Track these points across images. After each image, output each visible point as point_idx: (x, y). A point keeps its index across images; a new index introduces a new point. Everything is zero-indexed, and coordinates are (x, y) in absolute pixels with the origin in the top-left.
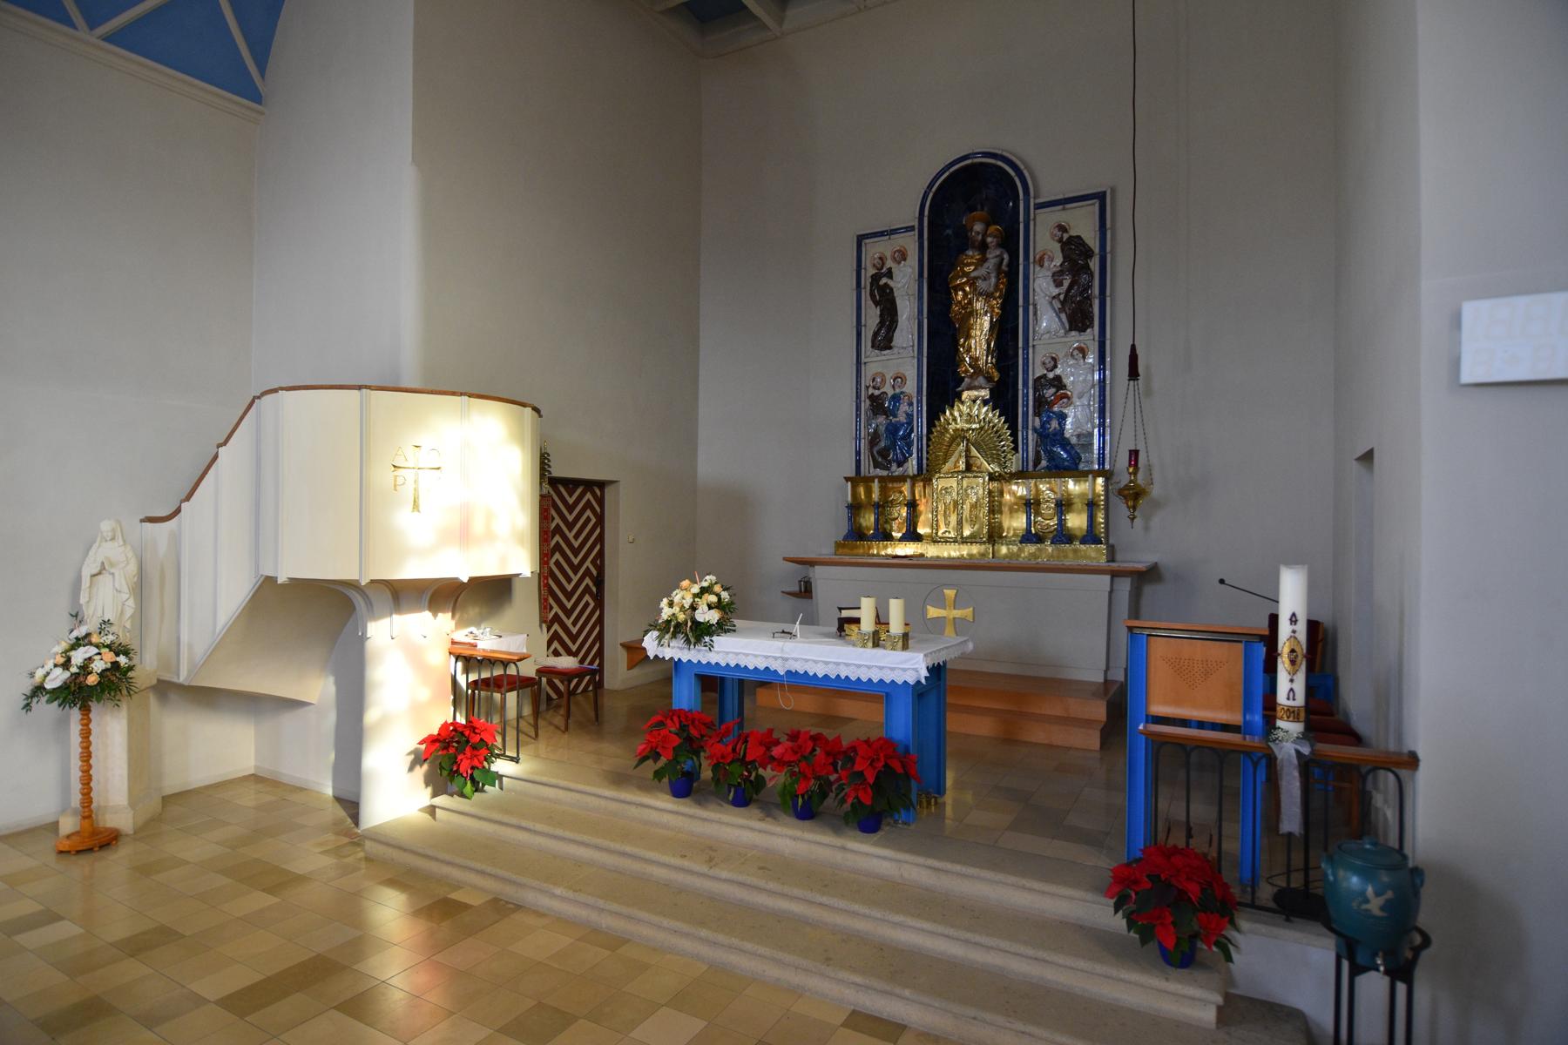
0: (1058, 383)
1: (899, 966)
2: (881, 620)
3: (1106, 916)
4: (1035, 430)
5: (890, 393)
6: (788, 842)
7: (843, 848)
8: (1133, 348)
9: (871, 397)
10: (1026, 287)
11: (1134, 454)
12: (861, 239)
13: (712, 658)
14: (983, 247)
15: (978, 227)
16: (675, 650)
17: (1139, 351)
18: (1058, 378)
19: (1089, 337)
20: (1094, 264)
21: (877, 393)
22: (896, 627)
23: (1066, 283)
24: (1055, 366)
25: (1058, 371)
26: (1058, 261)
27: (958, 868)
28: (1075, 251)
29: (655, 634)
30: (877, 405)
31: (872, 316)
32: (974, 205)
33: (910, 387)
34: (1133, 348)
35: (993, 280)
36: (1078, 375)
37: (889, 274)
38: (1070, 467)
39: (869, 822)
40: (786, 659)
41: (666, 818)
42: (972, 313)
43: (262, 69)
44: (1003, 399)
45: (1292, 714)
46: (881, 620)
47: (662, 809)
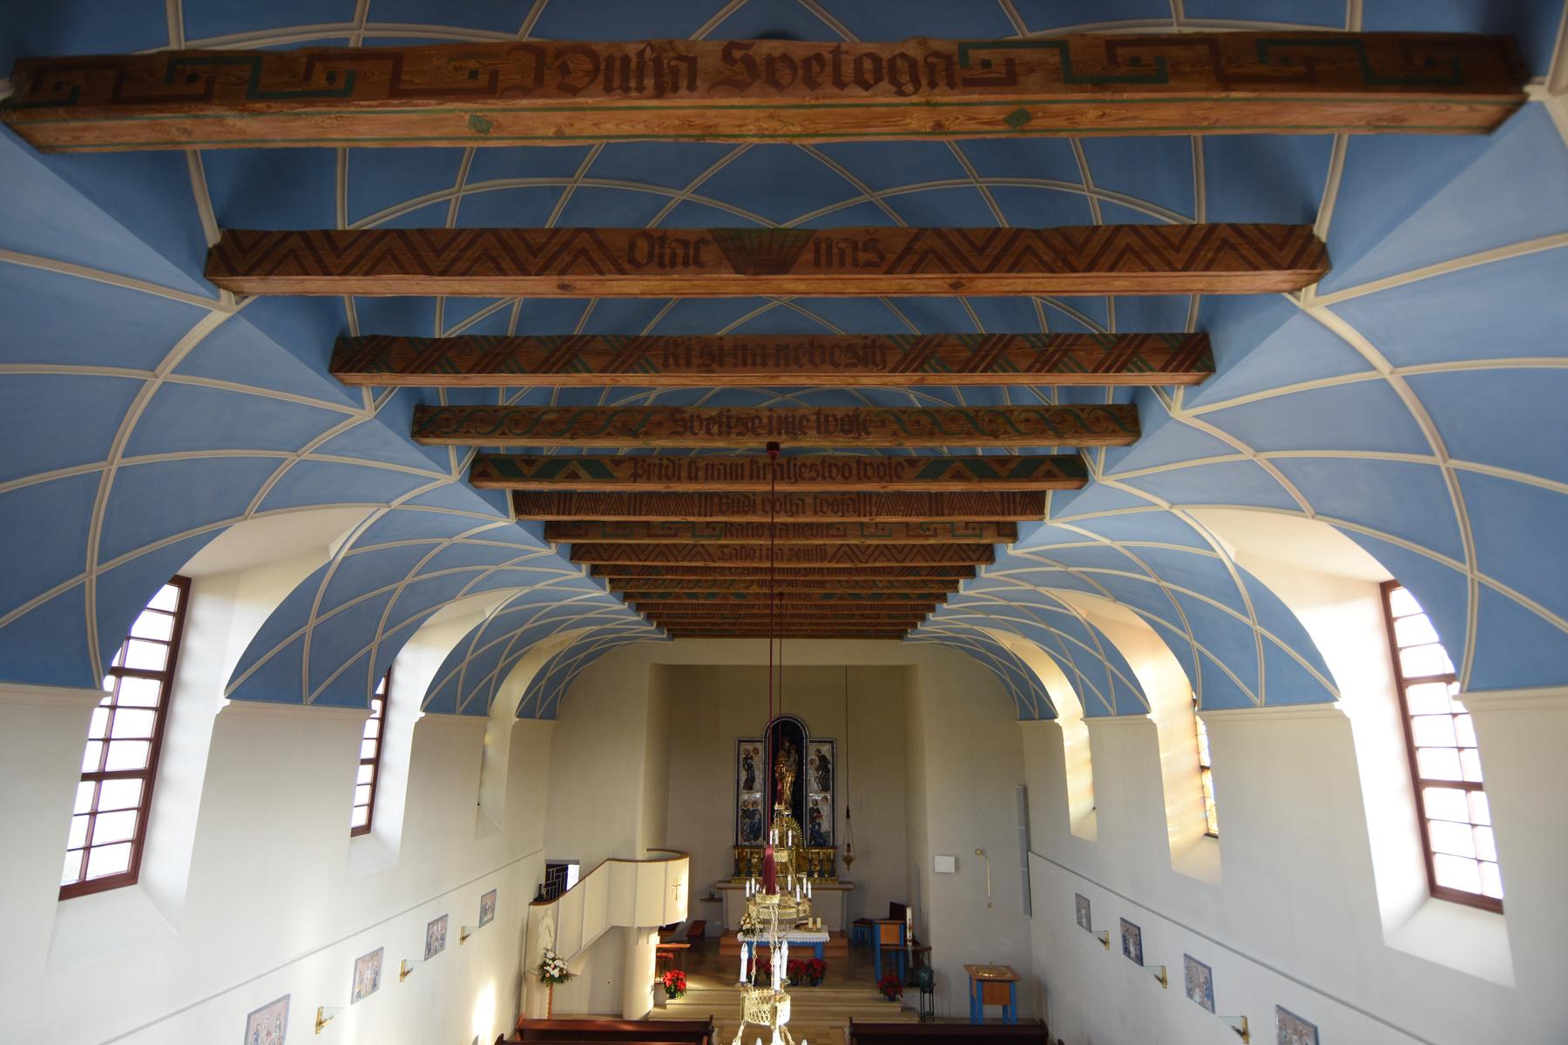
0: (818, 811)
3: (877, 994)
14: (789, 752)
22: (819, 925)
28: (823, 758)
30: (746, 813)
31: (744, 776)
32: (786, 736)
33: (760, 808)
36: (825, 810)
38: (822, 845)
39: (814, 983)
42: (783, 777)
43: (262, 509)
44: (797, 813)
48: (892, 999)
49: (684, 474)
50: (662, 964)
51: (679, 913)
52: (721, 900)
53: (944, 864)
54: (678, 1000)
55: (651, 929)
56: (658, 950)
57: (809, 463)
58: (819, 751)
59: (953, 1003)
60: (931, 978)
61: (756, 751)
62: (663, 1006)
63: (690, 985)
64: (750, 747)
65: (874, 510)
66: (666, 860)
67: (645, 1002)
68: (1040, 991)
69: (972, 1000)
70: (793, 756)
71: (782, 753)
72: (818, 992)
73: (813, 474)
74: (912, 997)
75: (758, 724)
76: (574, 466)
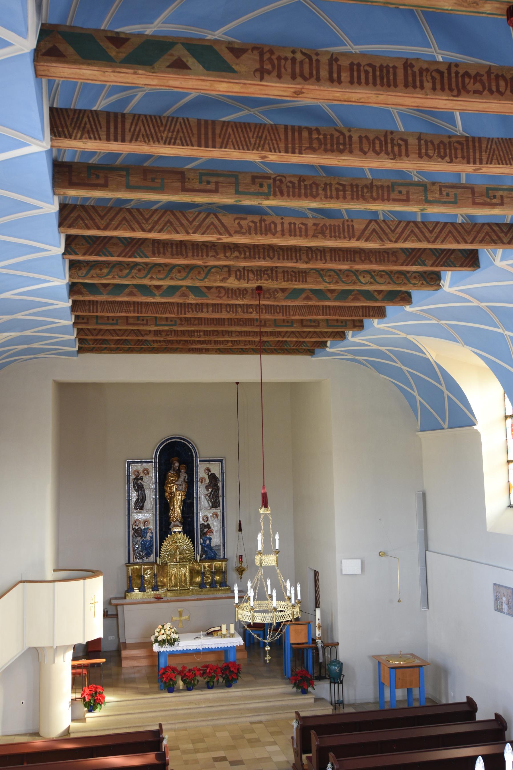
0: (208, 527)
1: (256, 711)
2: (228, 629)
3: (290, 688)
4: (201, 544)
5: (143, 528)
6: (211, 695)
7: (228, 692)
8: (240, 521)
9: (136, 531)
10: (197, 490)
11: (241, 557)
12: (129, 463)
13: (179, 649)
15: (177, 464)
16: (167, 648)
17: (241, 523)
18: (208, 525)
19: (219, 511)
20: (220, 484)
21: (137, 528)
23: (210, 490)
24: (207, 520)
25: (208, 522)
26: (207, 481)
27: (257, 688)
28: (213, 477)
29: (157, 644)
30: (139, 533)
31: (134, 495)
32: (176, 456)
33: (151, 526)
34: (240, 521)
35: (184, 486)
36: (215, 525)
37: (142, 479)
39: (229, 684)
40: (202, 645)
41: (170, 699)
42: (172, 495)
44: (189, 531)
45: (319, 638)
46: (228, 629)
47: (168, 698)
48: (305, 692)
49: (324, 73)
50: (76, 683)
51: (95, 630)
52: (116, 616)
53: (351, 566)
54: (97, 713)
55: (65, 648)
56: (74, 667)
57: (473, 73)
58: (209, 470)
59: (360, 690)
60: (341, 670)
61: (146, 472)
62: (84, 720)
63: (110, 698)
64: (139, 467)
65: (485, 157)
66: (84, 578)
67: (63, 716)
68: (442, 672)
69: (381, 686)
70: (183, 475)
71: (171, 473)
72: (234, 692)
73: (478, 86)
74: (323, 689)
75: (147, 448)
76: (180, 51)
